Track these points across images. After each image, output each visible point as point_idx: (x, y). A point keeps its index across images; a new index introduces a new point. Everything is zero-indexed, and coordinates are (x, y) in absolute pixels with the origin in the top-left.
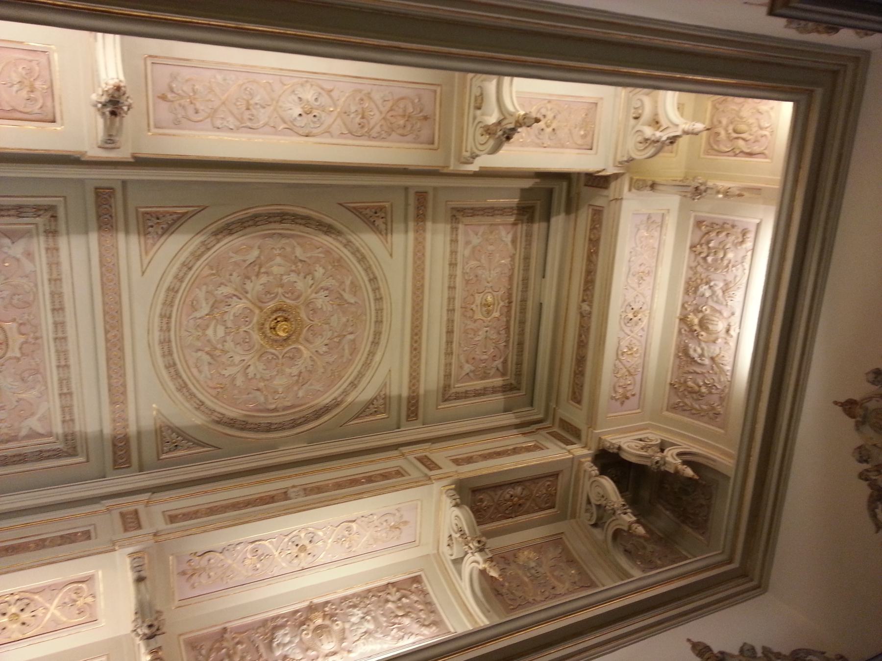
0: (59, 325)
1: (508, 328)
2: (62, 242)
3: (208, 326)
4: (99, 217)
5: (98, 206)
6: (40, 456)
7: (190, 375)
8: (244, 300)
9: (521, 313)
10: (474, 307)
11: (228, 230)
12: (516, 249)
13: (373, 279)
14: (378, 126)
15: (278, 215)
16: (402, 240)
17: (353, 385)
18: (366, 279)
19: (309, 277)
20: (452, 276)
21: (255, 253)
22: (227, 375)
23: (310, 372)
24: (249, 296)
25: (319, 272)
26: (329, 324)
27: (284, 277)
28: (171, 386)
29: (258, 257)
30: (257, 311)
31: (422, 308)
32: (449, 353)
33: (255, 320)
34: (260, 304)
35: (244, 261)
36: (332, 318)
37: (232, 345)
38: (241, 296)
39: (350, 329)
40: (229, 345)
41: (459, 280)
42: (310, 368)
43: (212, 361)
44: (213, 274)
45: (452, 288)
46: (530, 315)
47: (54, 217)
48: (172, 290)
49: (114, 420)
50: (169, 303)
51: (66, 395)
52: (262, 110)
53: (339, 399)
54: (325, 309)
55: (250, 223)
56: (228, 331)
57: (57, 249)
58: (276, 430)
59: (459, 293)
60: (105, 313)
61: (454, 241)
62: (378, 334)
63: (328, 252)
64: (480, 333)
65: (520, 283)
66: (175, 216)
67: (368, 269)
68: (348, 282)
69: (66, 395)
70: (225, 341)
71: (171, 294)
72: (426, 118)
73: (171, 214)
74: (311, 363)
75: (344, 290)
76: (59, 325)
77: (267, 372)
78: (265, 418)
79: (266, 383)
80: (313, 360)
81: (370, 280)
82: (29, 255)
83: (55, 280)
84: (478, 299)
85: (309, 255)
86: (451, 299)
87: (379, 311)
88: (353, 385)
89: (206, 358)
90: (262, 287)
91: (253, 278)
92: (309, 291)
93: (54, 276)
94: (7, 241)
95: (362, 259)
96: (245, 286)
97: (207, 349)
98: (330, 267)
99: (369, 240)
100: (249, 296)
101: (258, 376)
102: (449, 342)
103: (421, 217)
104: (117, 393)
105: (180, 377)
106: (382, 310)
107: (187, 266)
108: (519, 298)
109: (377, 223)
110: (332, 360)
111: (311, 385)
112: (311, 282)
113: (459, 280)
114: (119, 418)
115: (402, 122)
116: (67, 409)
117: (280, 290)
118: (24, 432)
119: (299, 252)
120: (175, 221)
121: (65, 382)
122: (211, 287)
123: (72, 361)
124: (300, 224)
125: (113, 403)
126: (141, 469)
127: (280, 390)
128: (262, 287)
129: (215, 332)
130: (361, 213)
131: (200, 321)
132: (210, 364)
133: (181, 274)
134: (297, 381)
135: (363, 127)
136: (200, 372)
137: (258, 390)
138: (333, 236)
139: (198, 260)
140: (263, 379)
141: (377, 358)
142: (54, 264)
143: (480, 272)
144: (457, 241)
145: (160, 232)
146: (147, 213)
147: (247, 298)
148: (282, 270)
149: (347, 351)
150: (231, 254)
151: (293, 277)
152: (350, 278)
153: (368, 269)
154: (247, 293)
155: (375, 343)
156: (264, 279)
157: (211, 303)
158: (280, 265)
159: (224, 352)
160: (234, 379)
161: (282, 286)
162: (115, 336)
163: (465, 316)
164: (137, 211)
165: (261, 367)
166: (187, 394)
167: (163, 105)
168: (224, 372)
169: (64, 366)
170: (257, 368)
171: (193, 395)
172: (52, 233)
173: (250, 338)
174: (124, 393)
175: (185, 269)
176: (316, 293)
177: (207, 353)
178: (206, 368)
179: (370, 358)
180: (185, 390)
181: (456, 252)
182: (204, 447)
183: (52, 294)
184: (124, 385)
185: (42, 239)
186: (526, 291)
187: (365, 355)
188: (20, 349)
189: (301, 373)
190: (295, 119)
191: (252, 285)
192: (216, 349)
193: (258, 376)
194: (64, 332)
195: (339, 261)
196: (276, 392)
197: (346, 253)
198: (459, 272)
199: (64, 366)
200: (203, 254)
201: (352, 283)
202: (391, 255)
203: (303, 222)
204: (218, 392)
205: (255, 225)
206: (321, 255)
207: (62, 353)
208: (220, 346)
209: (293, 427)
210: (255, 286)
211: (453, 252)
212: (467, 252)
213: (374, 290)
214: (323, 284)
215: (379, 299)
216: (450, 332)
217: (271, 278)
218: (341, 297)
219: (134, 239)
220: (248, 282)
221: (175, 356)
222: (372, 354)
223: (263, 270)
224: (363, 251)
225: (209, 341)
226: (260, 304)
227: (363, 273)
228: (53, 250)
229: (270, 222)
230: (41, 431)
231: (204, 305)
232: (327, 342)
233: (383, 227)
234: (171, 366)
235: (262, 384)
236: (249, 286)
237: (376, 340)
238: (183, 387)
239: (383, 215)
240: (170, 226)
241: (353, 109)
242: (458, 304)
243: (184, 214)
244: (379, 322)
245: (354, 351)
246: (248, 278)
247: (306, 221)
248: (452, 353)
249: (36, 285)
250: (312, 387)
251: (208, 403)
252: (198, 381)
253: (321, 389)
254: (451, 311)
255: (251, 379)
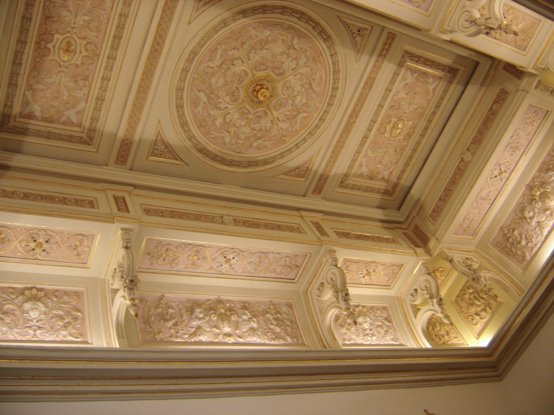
0: (369, 129)
1: (47, 18)
2: (345, 171)
3: (303, 105)
4: (325, 182)
5: (323, 187)
6: (419, 59)
7: (328, 78)
8: (276, 116)
9: (28, 30)
10: (84, 53)
11: (266, 162)
12: (24, 94)
13: (180, 107)
14: (186, 249)
15: (232, 165)
16: (146, 131)
17: (225, 23)
18: (185, 108)
19: (228, 120)
20: (103, 89)
21: (255, 144)
22: (308, 69)
23: (253, 48)
24: (272, 118)
25: (218, 122)
26: (225, 81)
27: (244, 124)
28: (341, 75)
29: (255, 140)
30: (271, 106)
31: (144, 73)
32: (123, 16)
33: (275, 100)
34: (267, 111)
35: (264, 141)
36: (221, 85)
37: (295, 89)
38: (276, 120)
39: (210, 70)
40: (298, 88)
41: (97, 83)
42: (253, 51)
43: (312, 81)
44: (285, 136)
45: (106, 79)
46: (18, 22)
47: (342, 182)
48: (311, 134)
49: (380, 68)
50: (317, 127)
51: (388, 90)
52: (253, 261)
53: (241, 16)
54: (225, 93)
55: (252, 164)
56: (294, 99)
57: (349, 167)
58: (297, 12)
59: (100, 71)
60: (349, 132)
61: (94, 119)
62: (190, 60)
63: (206, 134)
64: (82, 23)
65: (24, 62)
66: (289, 174)
67: (181, 116)
68: (200, 108)
69: (388, 90)
70: (298, 92)
71: (313, 133)
72: (149, 254)
73: (290, 175)
74: (251, 56)
75: (205, 103)
76: (369, 129)
77: (283, 60)
78: (301, 26)
79: (287, 52)
80: (248, 55)
81: (182, 107)
82: (361, 165)
83: (358, 152)
84: (77, 59)
85: (222, 135)
86: (109, 68)
87: (182, 80)
88: (225, 23)
89: (314, 86)
90: (260, 121)
91: (264, 129)
92: (231, 111)
93: (357, 154)
94: (365, 174)
95: (184, 125)
96: (270, 124)
97: (311, 91)
98: (209, 123)
99: (174, 136)
100: (272, 118)
101: (290, 59)
102: (120, 27)
103: (126, 146)
104: (369, 85)
105: (334, 79)
106: (179, 80)
107: (297, 146)
108: (28, 45)
109: (163, 147)
110: (233, 51)
111: (257, 36)
112: (228, 117)
113: (97, 83)
114: (377, 68)
115: (169, 252)
116: (392, 82)
117: (250, 117)
118: (416, 75)
119: (227, 140)
120: (291, 172)
121: (385, 98)
122: (290, 129)
123: (376, 107)
124: (220, 157)
125: (374, 79)
126: (383, 28)
127: (280, 42)
128: (260, 121)
129: (301, 101)
130: (174, 156)
131: (305, 110)
132: (314, 80)
133: (303, 142)
134: (266, 44)
135: (196, 251)
136: (321, 77)
137: (294, 48)
138: (200, 145)
139: (290, 148)
140: (288, 56)
141: (198, 39)
142: (354, 160)
143: (71, 84)
144: (92, 118)
145: (300, 168)
146: (301, 177)
147: (274, 118)
148: (244, 130)
149: (219, 54)
150: (270, 146)
151: (239, 123)
152: (196, 111)
153: (181, 116)
154: (272, 120)
155: (194, 53)
156: (257, 126)
157: (295, 119)
158: (244, 133)
159: (302, 86)
160: (305, 63)
161: (247, 118)
162: (352, 118)
163: (96, 45)
164: (306, 180)
165: (285, 66)
166: (336, 67)
167: (298, 264)
168: (309, 70)
169: (381, 106)
170: (288, 65)
171: (334, 64)
172: (346, 176)
173: (283, 89)
174: (366, 83)
175: (299, 145)
176: (227, 108)
177: (312, 88)
178: (317, 78)
179: (203, 42)
180: (336, 70)
181: (95, 109)
182: (345, 22)
183: (363, 146)
184: (364, 88)
185: (352, 173)
186: (17, 52)
187: (207, 45)
188: (390, 122)
189: (261, 49)
190: (236, 256)
191: (267, 125)
192: (306, 90)
193: (290, 59)
194: (370, 125)
195: (201, 126)
196: (284, 41)
197: (195, 130)
198: (95, 92)
199: (381, 106)
200: (286, 152)
201: (196, 108)
202: (159, 122)
203: (218, 158)
204: (318, 57)
205: (249, 162)
206: (211, 132)
207: (377, 114)
208: (303, 90)
209: (285, 8)
210: (266, 123)
211: (97, 109)
212: (82, 105)
213: (182, 98)
214: (220, 112)
215: (180, 90)
216: (118, 37)
217: (253, 126)
218: (209, 98)
219: (315, 168)
220: (268, 128)
221: (330, 94)
222: (200, 45)
223: (256, 132)
224: (181, 130)
225: (307, 95)
226: (267, 111)
227: (186, 113)
228: (351, 167)
229: (239, 162)
230: (409, 73)
231: (298, 121)
232: (232, 67)
233: (159, 144)
234: (335, 89)
235: (291, 51)
236: (269, 124)
237: (192, 55)
238: (336, 72)
239: (156, 151)
240: (294, 170)
241: (200, 261)
242: (103, 61)
243: (284, 174)
244: (185, 71)
245: (214, 51)
246: (267, 130)
247: (215, 158)
248: (121, 15)
249: (367, 151)
250: (257, 34)
251: (328, 54)
252: (326, 71)
253: (250, 29)
254: (111, 58)
255: (295, 59)
